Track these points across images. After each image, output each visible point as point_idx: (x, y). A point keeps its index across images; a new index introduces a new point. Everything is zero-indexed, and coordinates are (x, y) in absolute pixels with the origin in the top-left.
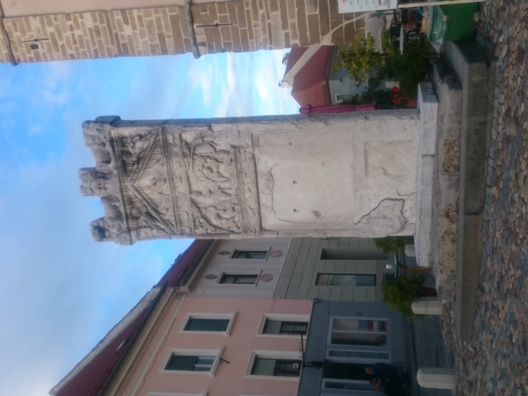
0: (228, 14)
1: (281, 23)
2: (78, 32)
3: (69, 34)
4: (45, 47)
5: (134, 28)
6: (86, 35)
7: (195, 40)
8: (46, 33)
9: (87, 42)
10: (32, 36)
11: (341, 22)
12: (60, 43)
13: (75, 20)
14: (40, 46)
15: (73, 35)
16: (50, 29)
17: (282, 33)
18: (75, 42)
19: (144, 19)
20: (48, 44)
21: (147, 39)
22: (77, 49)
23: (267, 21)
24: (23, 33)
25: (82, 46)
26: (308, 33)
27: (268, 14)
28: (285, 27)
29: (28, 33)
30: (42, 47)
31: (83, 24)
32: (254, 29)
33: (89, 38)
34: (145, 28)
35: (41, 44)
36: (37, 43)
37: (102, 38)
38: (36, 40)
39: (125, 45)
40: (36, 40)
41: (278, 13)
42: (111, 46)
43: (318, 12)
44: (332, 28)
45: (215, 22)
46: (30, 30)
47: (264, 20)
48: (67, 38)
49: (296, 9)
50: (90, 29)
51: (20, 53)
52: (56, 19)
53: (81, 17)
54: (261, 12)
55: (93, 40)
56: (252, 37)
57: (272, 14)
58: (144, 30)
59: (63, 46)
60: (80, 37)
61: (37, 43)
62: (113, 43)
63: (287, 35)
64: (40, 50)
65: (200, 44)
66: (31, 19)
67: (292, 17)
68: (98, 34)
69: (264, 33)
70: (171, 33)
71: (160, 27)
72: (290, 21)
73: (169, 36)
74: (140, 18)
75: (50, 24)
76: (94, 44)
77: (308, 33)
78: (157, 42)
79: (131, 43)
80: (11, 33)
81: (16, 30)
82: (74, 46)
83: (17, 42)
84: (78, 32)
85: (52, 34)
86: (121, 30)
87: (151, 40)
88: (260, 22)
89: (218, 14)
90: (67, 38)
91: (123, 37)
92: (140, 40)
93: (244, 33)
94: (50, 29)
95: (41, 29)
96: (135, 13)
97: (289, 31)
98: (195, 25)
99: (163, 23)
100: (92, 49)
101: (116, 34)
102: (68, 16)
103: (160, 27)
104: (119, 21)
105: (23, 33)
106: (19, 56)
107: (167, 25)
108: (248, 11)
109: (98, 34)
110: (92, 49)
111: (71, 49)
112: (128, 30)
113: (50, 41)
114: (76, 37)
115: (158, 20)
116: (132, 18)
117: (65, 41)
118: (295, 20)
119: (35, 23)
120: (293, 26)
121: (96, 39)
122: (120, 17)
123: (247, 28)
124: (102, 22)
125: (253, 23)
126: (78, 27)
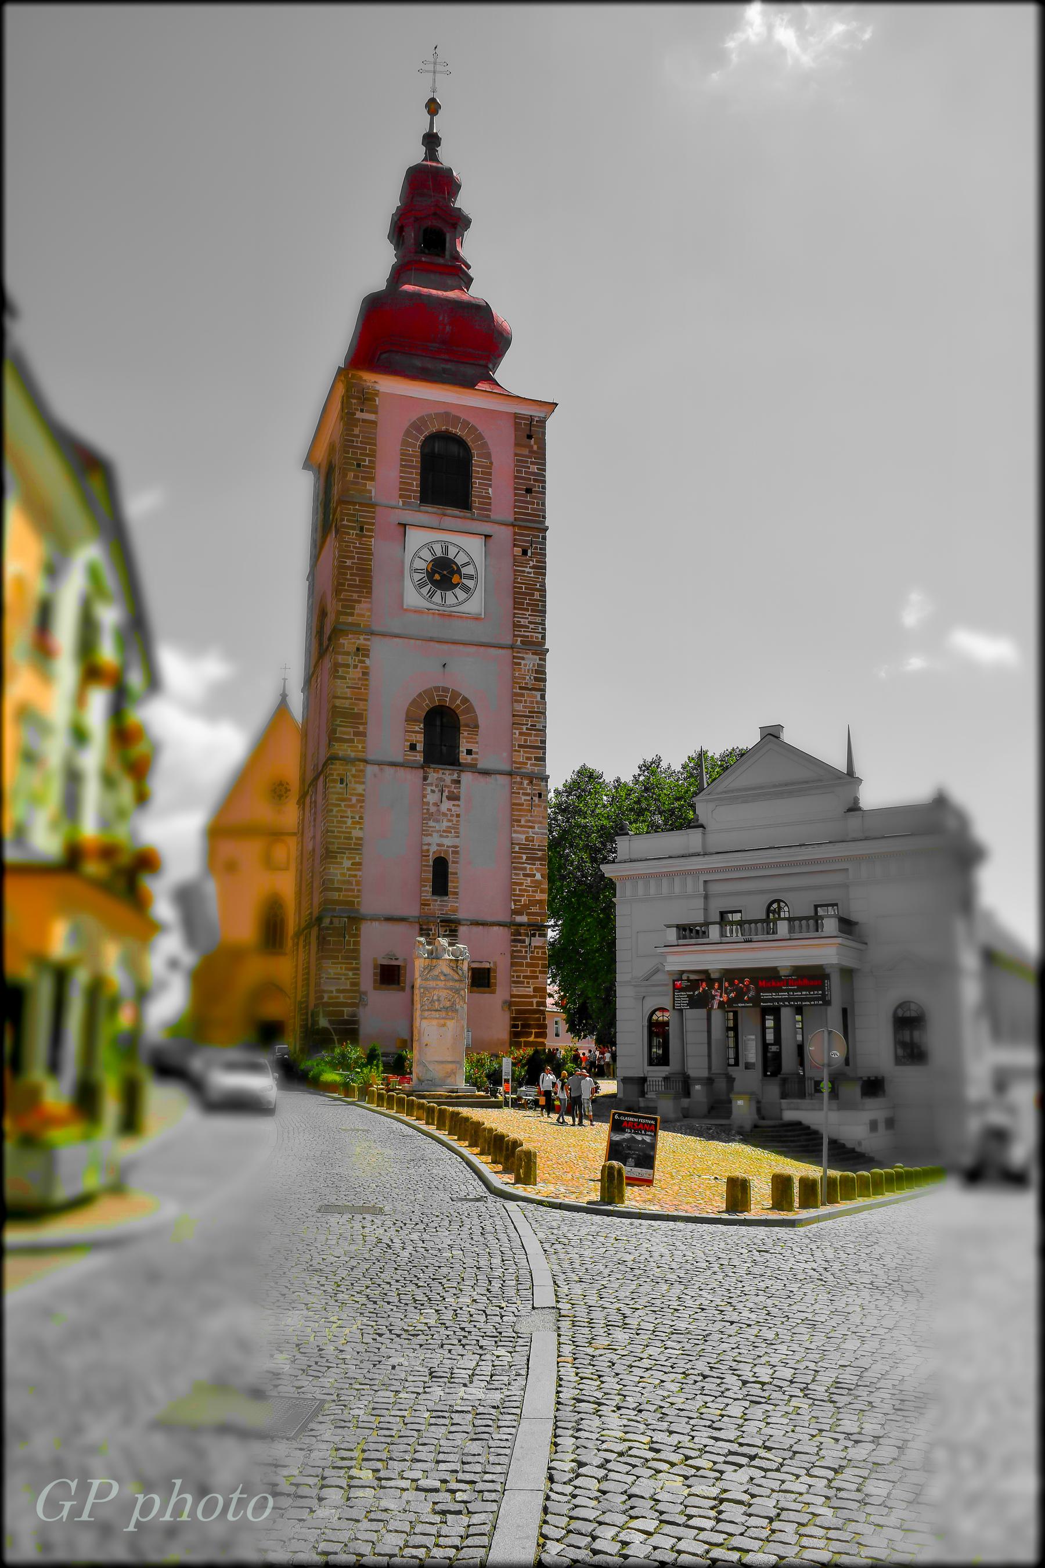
0: (352, 947)
1: (341, 988)
2: (349, 821)
3: (349, 814)
4: (341, 791)
5: (349, 869)
6: (346, 828)
7: (335, 917)
8: (351, 795)
9: (342, 827)
10: (350, 783)
11: (336, 1035)
12: (343, 804)
13: (359, 823)
14: (342, 785)
15: (348, 817)
16: (354, 799)
17: (333, 988)
18: (342, 817)
19: (354, 879)
20: (342, 794)
21: (339, 877)
22: (336, 817)
23: (343, 977)
24: (354, 776)
25: (339, 822)
26: (331, 1009)
27: (348, 979)
28: (338, 991)
29: (353, 780)
30: (341, 788)
31: (355, 828)
32: (339, 966)
33: (344, 830)
34: (347, 878)
35: (343, 788)
36: (345, 784)
37: (342, 841)
38: (347, 785)
39: (336, 857)
40: (347, 785)
41: (348, 987)
42: (336, 846)
43: (345, 1017)
44: (333, 1028)
45: (347, 936)
46: (356, 782)
47: (344, 975)
48: (345, 811)
49: (349, 1001)
50: (350, 833)
51: (338, 767)
52: (361, 807)
53: (361, 829)
54: (350, 973)
55: (343, 832)
56: (333, 963)
57: (348, 982)
58: (346, 877)
59: (340, 805)
60: (345, 823)
61: (345, 784)
62: (338, 848)
63: (332, 992)
64: (339, 785)
65: (331, 920)
66: (363, 787)
67: (344, 997)
68: (346, 838)
69: (335, 974)
70: (341, 898)
71: (347, 890)
72: (342, 995)
73: (339, 895)
74: (355, 876)
75: (359, 801)
76: (339, 832)
77: (331, 1009)
78: (336, 885)
79: (337, 863)
80: (355, 766)
81: (356, 771)
82: (339, 815)
83: (347, 767)
84: (349, 821)
85: (350, 800)
86: (349, 858)
87: (338, 880)
88: (344, 971)
89: (352, 940)
90: (345, 811)
91: (342, 858)
92: (338, 872)
93: (337, 958)
94: (354, 799)
95: (355, 792)
96: (359, 873)
97: (335, 994)
98: (346, 920)
99: (350, 893)
100: (336, 830)
101: (345, 853)
102: (361, 818)
103: (347, 890)
104: (354, 858)
105: (354, 776)
106: (335, 764)
107: (348, 896)
108: (352, 964)
109: (346, 838)
110: (336, 830)
111: (337, 811)
112: (347, 863)
113: (345, 796)
114: (346, 819)
115: (353, 890)
116: (356, 870)
117: (344, 808)
118: (342, 1000)
119: (360, 788)
120: (337, 997)
121: (343, 835)
122: (357, 860)
123: (340, 960)
124: (355, 844)
125: (344, 966)
126: (353, 823)
